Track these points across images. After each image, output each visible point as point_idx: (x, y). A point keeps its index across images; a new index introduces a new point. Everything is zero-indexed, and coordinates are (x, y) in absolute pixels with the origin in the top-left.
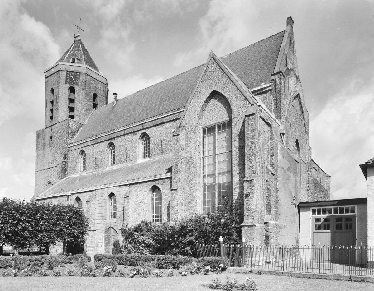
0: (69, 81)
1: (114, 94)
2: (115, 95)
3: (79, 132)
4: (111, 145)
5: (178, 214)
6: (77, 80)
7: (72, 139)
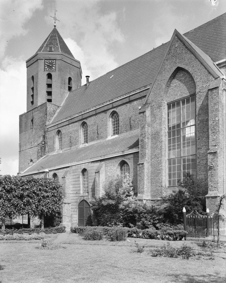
0: (47, 68)
1: (87, 77)
2: (88, 78)
3: (56, 114)
4: (84, 124)
5: (145, 186)
6: (54, 67)
7: (50, 121)
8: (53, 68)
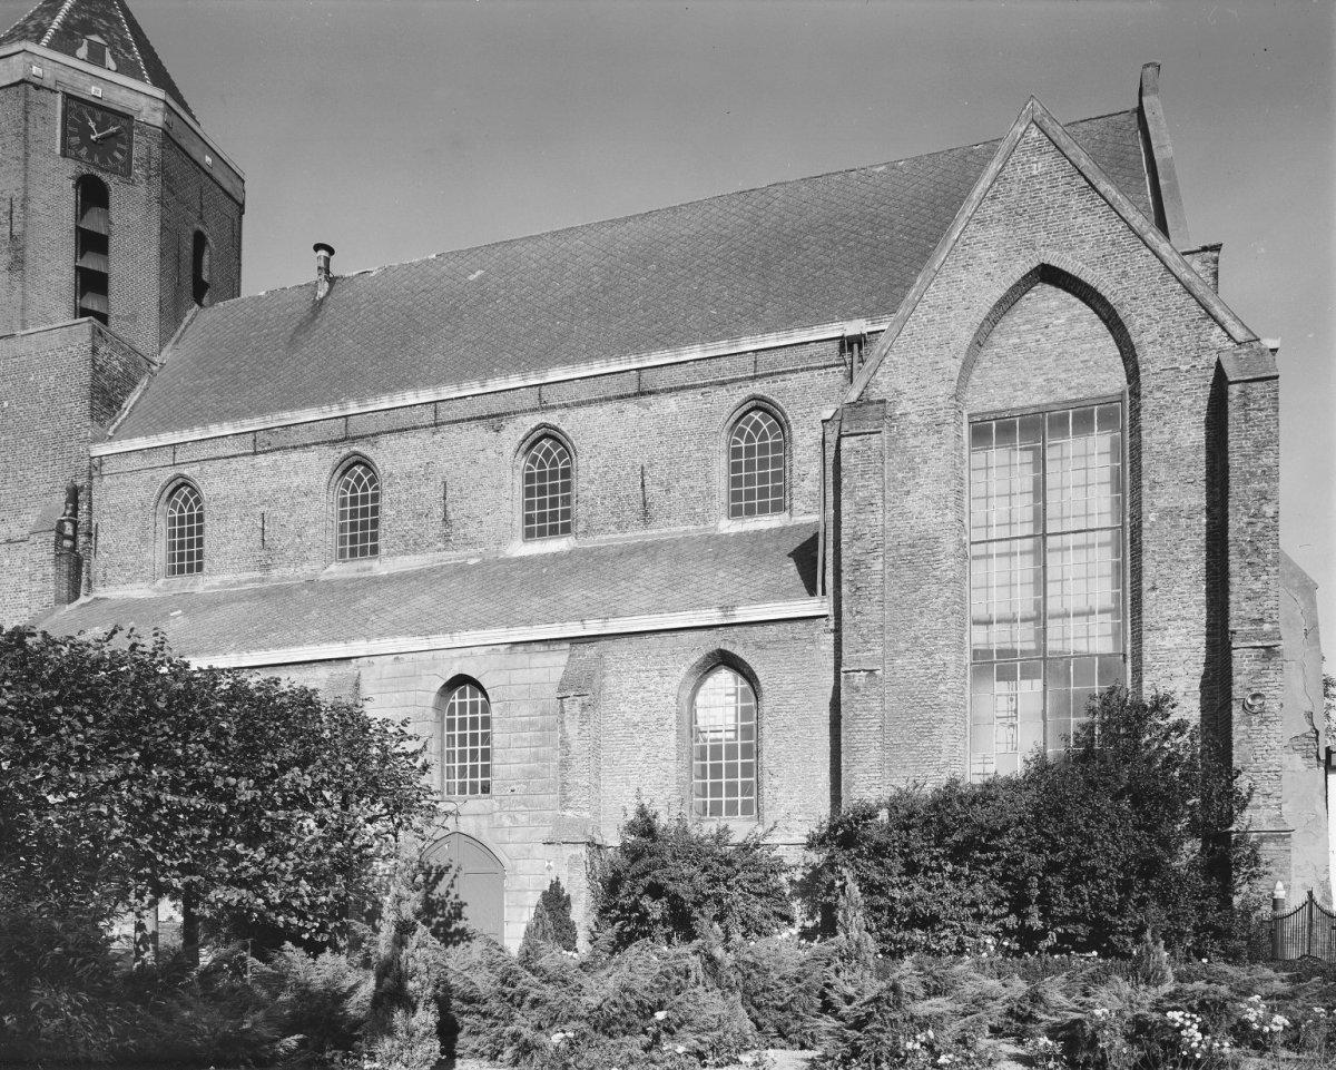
6: (121, 152)
8: (118, 155)
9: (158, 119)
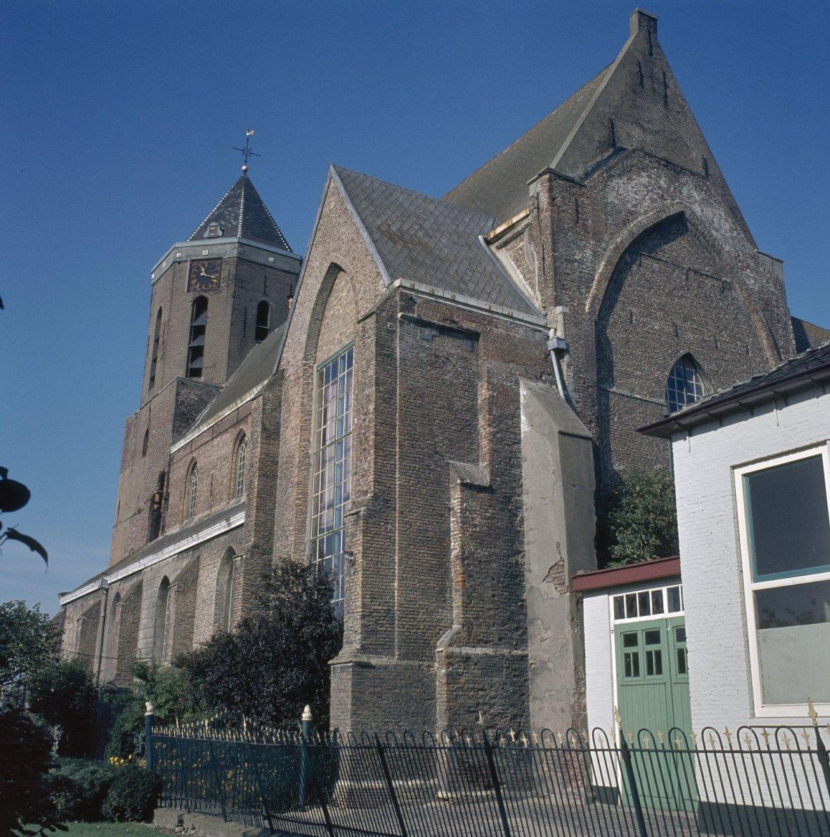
9: (235, 253)
